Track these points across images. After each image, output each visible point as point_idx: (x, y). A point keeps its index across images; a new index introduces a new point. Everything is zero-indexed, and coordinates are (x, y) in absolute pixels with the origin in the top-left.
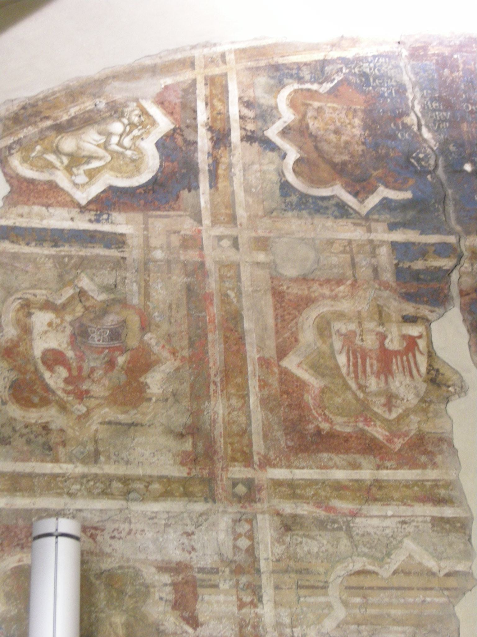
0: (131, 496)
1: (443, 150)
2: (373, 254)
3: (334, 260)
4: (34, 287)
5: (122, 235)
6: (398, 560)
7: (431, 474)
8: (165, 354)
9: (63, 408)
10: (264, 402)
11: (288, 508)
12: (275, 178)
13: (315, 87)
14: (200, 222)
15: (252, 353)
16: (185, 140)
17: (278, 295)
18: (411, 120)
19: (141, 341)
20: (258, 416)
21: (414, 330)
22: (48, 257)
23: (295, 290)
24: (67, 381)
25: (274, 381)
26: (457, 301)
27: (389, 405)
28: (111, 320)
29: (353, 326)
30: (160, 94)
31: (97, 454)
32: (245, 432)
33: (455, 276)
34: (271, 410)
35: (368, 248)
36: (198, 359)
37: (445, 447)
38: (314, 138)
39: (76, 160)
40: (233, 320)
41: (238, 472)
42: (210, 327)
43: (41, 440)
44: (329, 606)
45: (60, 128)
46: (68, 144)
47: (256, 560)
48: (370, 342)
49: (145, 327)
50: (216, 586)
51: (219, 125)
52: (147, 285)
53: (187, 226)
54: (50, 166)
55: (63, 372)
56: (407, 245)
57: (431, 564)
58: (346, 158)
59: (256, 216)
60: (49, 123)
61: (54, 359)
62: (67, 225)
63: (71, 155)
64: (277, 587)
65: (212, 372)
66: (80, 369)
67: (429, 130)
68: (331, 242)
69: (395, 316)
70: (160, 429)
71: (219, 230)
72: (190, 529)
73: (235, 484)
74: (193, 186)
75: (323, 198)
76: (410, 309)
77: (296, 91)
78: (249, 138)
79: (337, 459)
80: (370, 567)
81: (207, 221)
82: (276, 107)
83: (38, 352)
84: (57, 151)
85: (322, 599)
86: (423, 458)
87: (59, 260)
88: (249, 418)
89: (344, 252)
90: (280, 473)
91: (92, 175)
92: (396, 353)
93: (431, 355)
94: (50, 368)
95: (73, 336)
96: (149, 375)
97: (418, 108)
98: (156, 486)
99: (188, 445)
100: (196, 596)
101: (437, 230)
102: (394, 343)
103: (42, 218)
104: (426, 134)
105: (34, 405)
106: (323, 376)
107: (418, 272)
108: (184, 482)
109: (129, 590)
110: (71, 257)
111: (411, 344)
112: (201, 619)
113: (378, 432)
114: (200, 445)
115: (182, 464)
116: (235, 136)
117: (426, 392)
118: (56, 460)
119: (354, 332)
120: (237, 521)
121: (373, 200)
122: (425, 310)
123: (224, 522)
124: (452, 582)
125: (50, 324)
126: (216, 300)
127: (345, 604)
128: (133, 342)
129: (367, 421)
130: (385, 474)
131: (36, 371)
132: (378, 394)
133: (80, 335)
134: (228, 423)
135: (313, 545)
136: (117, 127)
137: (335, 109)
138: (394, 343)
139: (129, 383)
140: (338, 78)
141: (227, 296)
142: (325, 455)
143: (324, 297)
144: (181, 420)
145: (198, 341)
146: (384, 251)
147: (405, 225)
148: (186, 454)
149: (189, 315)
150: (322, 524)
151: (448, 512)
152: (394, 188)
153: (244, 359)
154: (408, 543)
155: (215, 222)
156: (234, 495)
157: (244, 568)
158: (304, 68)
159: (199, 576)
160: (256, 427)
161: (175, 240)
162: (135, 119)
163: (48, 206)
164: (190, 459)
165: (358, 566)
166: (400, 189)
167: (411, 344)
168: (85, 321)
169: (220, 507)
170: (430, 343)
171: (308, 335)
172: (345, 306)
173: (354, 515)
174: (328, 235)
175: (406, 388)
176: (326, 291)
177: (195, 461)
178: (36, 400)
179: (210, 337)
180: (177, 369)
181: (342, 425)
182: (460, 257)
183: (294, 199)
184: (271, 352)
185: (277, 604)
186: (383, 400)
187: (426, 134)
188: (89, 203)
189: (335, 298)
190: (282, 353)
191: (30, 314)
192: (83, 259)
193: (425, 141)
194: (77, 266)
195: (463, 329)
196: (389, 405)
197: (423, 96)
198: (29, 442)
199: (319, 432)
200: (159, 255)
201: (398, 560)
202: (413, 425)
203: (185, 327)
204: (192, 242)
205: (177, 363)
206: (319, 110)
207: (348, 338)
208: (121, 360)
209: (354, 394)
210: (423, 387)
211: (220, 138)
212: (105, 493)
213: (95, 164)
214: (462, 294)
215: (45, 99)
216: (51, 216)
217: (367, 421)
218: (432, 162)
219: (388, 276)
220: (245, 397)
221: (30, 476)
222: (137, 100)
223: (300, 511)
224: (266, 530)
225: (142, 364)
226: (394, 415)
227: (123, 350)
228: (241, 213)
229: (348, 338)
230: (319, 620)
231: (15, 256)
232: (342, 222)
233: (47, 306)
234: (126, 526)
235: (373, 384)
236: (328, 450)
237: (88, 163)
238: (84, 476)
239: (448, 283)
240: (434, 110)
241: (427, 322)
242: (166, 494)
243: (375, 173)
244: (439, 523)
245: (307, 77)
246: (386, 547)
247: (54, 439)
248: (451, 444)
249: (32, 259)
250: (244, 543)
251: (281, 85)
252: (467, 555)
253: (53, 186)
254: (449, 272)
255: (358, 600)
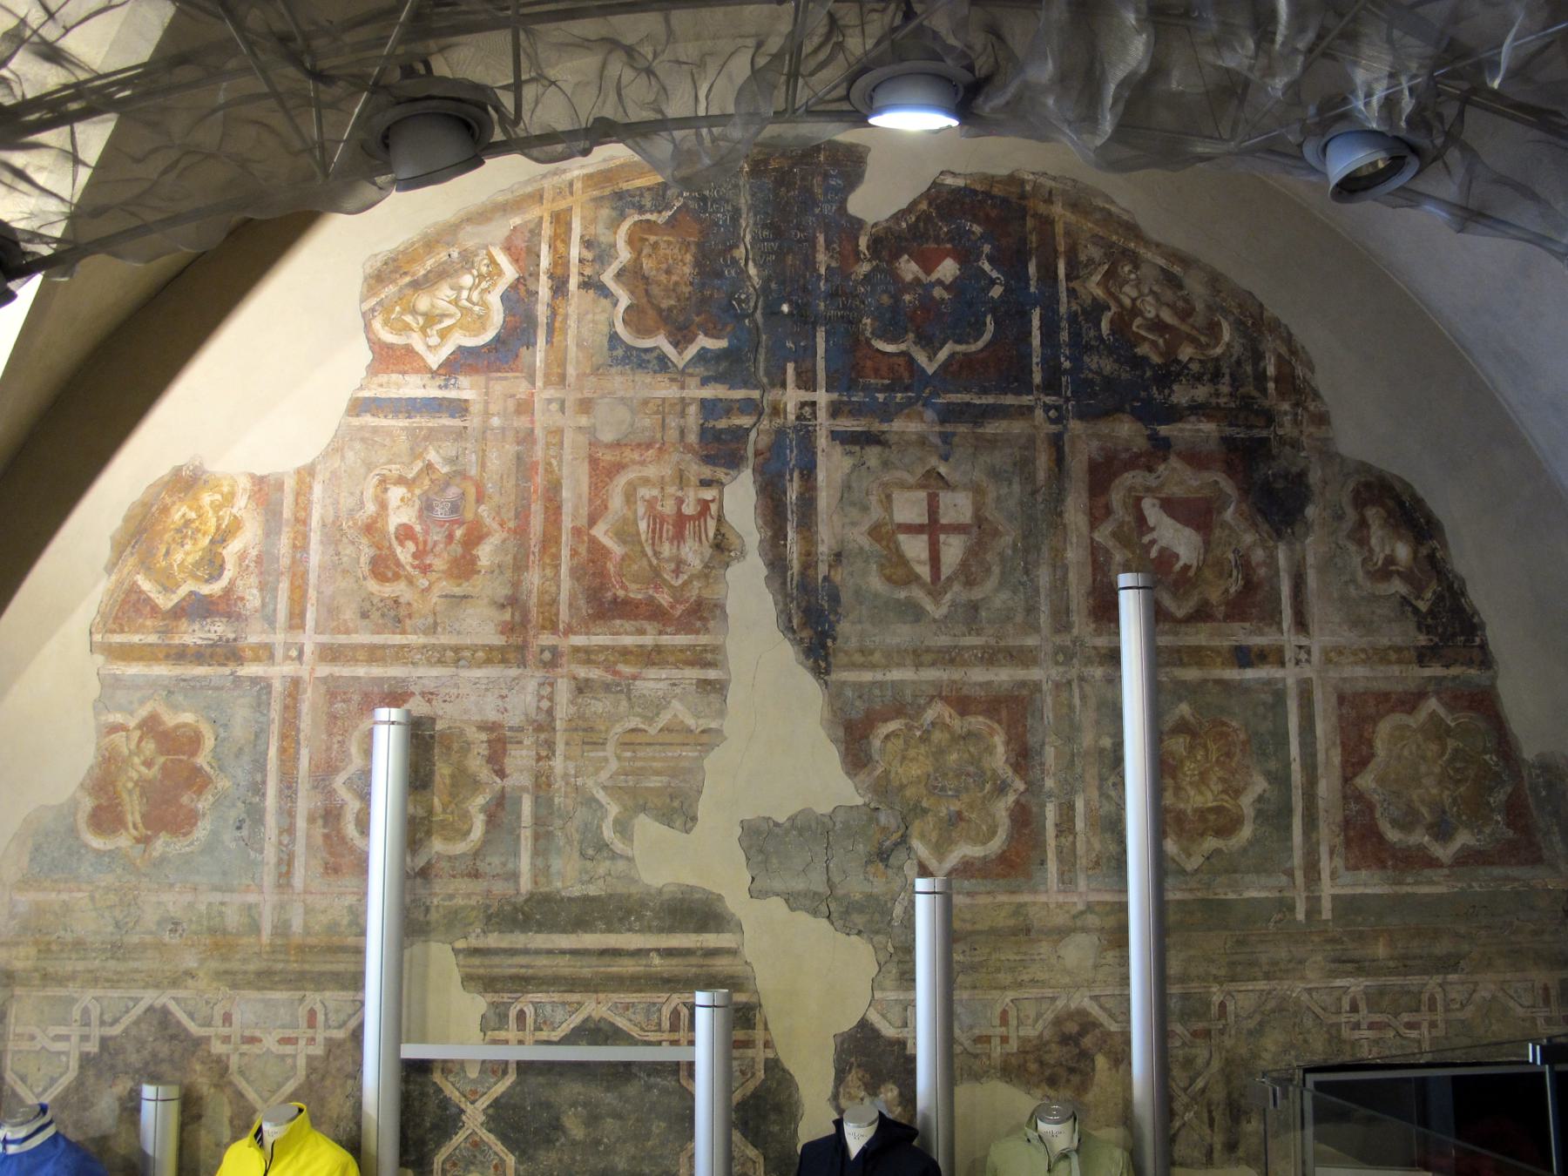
0: (462, 663)
1: (765, 290)
2: (683, 414)
3: (647, 422)
4: (390, 462)
5: (466, 401)
6: (665, 718)
7: (703, 639)
8: (495, 526)
9: (410, 581)
10: (573, 572)
11: (582, 672)
12: (606, 330)
13: (653, 217)
14: (533, 384)
15: (567, 523)
16: (528, 291)
17: (594, 461)
18: (740, 253)
19: (476, 514)
20: (566, 584)
21: (708, 494)
22: (403, 429)
23: (608, 457)
24: (415, 556)
25: (583, 550)
26: (751, 462)
27: (677, 572)
28: (453, 492)
29: (655, 492)
30: (509, 239)
31: (436, 624)
32: (554, 601)
33: (753, 435)
34: (578, 580)
35: (678, 408)
36: (521, 531)
37: (718, 612)
38: (645, 278)
39: (431, 319)
40: (553, 490)
41: (547, 639)
42: (534, 497)
43: (392, 613)
44: (606, 760)
45: (416, 285)
46: (423, 303)
47: (553, 720)
48: (669, 508)
49: (480, 500)
50: (520, 742)
51: (559, 271)
52: (484, 456)
53: (522, 388)
54: (408, 328)
55: (411, 547)
56: (716, 401)
57: (691, 722)
58: (672, 302)
59: (584, 374)
60: (407, 279)
61: (406, 533)
62: (420, 393)
63: (425, 315)
64: (567, 744)
65: (532, 543)
66: (425, 542)
67: (755, 265)
68: (646, 402)
69: (694, 480)
70: (486, 601)
71: (551, 393)
72: (504, 692)
73: (542, 651)
74: (530, 344)
75: (647, 350)
76: (707, 472)
77: (635, 224)
78: (586, 285)
79: (629, 625)
80: (642, 726)
81: (539, 384)
82: (614, 246)
83: (392, 529)
84: (414, 311)
85: (601, 754)
86: (698, 624)
87: (412, 433)
88: (559, 587)
89: (656, 413)
90: (578, 640)
91: (443, 334)
92: (690, 518)
93: (720, 519)
94: (401, 544)
95: (421, 510)
96: (480, 547)
97: (748, 238)
98: (480, 654)
99: (507, 616)
100: (505, 751)
101: (746, 384)
102: (689, 509)
103: (399, 386)
104: (752, 271)
105: (388, 580)
106: (624, 542)
107: (721, 431)
108: (502, 650)
109: (455, 746)
110: (421, 428)
111: (705, 506)
112: (508, 771)
113: (664, 599)
114: (517, 617)
115: (502, 633)
116: (573, 282)
117: (712, 557)
118: (404, 632)
119: (655, 498)
120: (541, 685)
121: (692, 351)
122: (720, 473)
123: (532, 685)
124: (705, 738)
125: (402, 499)
126: (541, 470)
127: (619, 758)
128: (469, 516)
129: (656, 588)
130: (666, 640)
131: (390, 547)
132: (668, 560)
133: (427, 507)
134: (542, 593)
135: (599, 706)
136: (467, 280)
137: (669, 243)
138: (689, 509)
139: (463, 557)
140: (678, 204)
141: (550, 464)
142: (618, 622)
143: (633, 462)
144: (503, 591)
145: (523, 515)
146: (693, 410)
147: (718, 379)
148: (505, 623)
149: (517, 485)
150: (607, 687)
151: (712, 674)
152: (713, 336)
153: (560, 529)
154: (676, 704)
155: (547, 383)
156: (541, 661)
157: (543, 725)
158: (647, 194)
159: (509, 734)
160: (564, 597)
161: (511, 404)
162: (484, 270)
163: (404, 373)
164: (508, 629)
165: (632, 725)
166: (718, 338)
167: (705, 506)
168: (431, 495)
169: (528, 672)
170: (721, 507)
171: (616, 502)
172: (651, 471)
173: (635, 678)
174: (646, 393)
175: (693, 553)
176: (636, 456)
177: (512, 630)
178: (390, 574)
179: (533, 507)
180: (504, 541)
181: (636, 593)
182: (761, 414)
183: (620, 352)
184: (583, 521)
185: (567, 758)
186: (673, 566)
187: (752, 271)
188: (440, 366)
189: (643, 463)
190: (592, 521)
191: (386, 490)
192: (431, 429)
193: (749, 277)
194: (426, 438)
195: (752, 491)
196: (677, 572)
197: (755, 224)
198: (383, 615)
199: (615, 598)
200: (496, 422)
201: (665, 718)
202: (693, 592)
203: (513, 497)
204: (524, 407)
205: (505, 535)
206: (655, 246)
207: (651, 504)
208: (459, 533)
209: (649, 561)
210: (708, 552)
211: (559, 287)
212: (441, 662)
213: (447, 322)
214: (757, 454)
215: (404, 252)
216: (407, 384)
217: (656, 588)
218: (752, 304)
219: (692, 438)
220: (557, 567)
221: (384, 647)
222: (486, 247)
223: (591, 675)
224: (564, 690)
225: (475, 536)
226: (680, 582)
227: (460, 523)
228: (571, 371)
229: (651, 504)
230: (597, 771)
231: (375, 430)
232: (659, 377)
233: (401, 481)
234: (455, 691)
235: (667, 550)
236: (621, 617)
237: (440, 322)
238: (424, 646)
239: (746, 443)
240: (764, 240)
241: (722, 485)
242: (488, 661)
243: (697, 319)
244: (704, 684)
245: (648, 205)
246: (659, 705)
247: (403, 612)
248: (723, 608)
249: (388, 432)
250: (545, 704)
251: (622, 216)
252: (721, 713)
253: (409, 350)
254: (748, 431)
255: (629, 754)
